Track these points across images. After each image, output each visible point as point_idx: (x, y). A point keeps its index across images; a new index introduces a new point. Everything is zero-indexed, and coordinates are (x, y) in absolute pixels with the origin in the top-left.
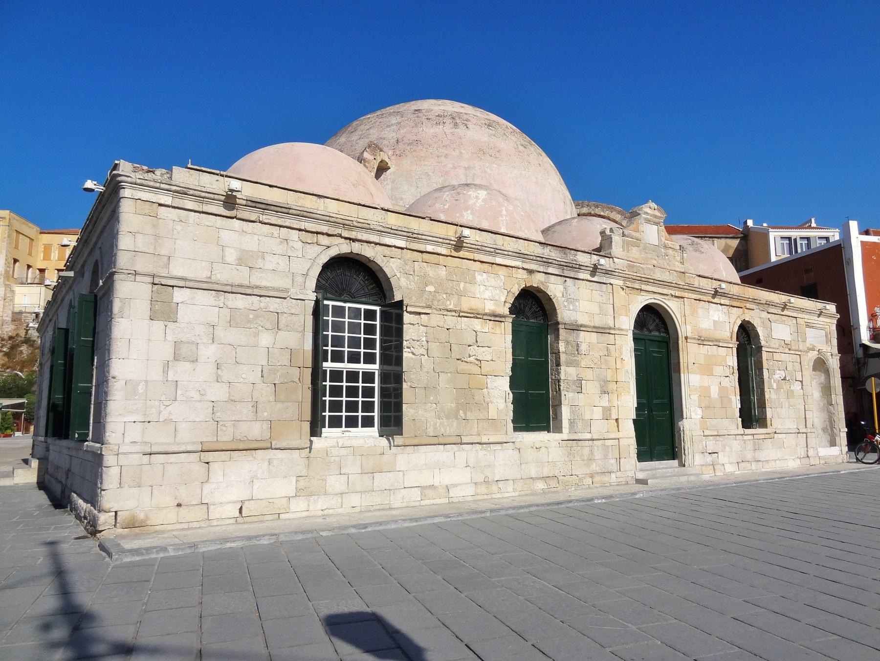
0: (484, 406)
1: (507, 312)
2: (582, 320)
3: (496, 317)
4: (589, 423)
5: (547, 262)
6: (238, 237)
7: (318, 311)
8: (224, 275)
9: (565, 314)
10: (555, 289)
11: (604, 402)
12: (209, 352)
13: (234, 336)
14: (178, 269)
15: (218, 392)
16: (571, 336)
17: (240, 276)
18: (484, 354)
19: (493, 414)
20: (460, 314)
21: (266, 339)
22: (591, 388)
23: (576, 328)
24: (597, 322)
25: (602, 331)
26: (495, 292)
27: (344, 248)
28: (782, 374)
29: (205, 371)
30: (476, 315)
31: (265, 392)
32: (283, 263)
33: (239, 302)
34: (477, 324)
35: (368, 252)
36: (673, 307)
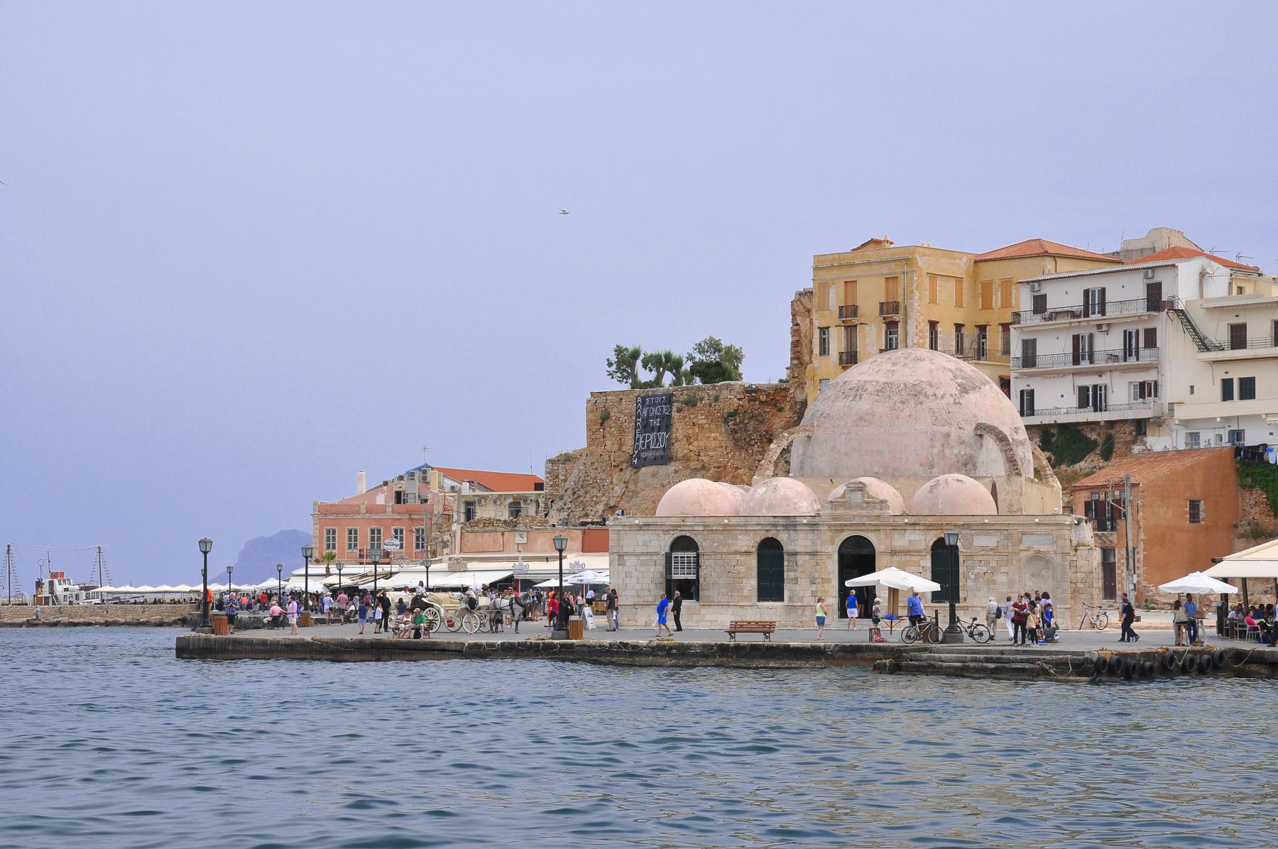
0: (742, 589)
1: (754, 550)
2: (799, 549)
3: (748, 553)
4: (801, 599)
5: (776, 525)
6: (643, 537)
7: (668, 557)
8: (639, 550)
9: (787, 547)
10: (782, 537)
11: (814, 588)
12: (635, 574)
13: (643, 569)
14: (625, 550)
15: (638, 587)
16: (792, 558)
17: (644, 550)
18: (742, 569)
19: (745, 593)
20: (729, 554)
21: (652, 569)
22: (803, 582)
23: (795, 554)
24: (809, 550)
25: (813, 554)
26: (749, 542)
27: (679, 534)
28: (985, 569)
29: (634, 580)
30: (736, 553)
31: (652, 586)
32: (657, 543)
33: (643, 558)
34: (738, 557)
35: (688, 534)
36: (871, 537)
